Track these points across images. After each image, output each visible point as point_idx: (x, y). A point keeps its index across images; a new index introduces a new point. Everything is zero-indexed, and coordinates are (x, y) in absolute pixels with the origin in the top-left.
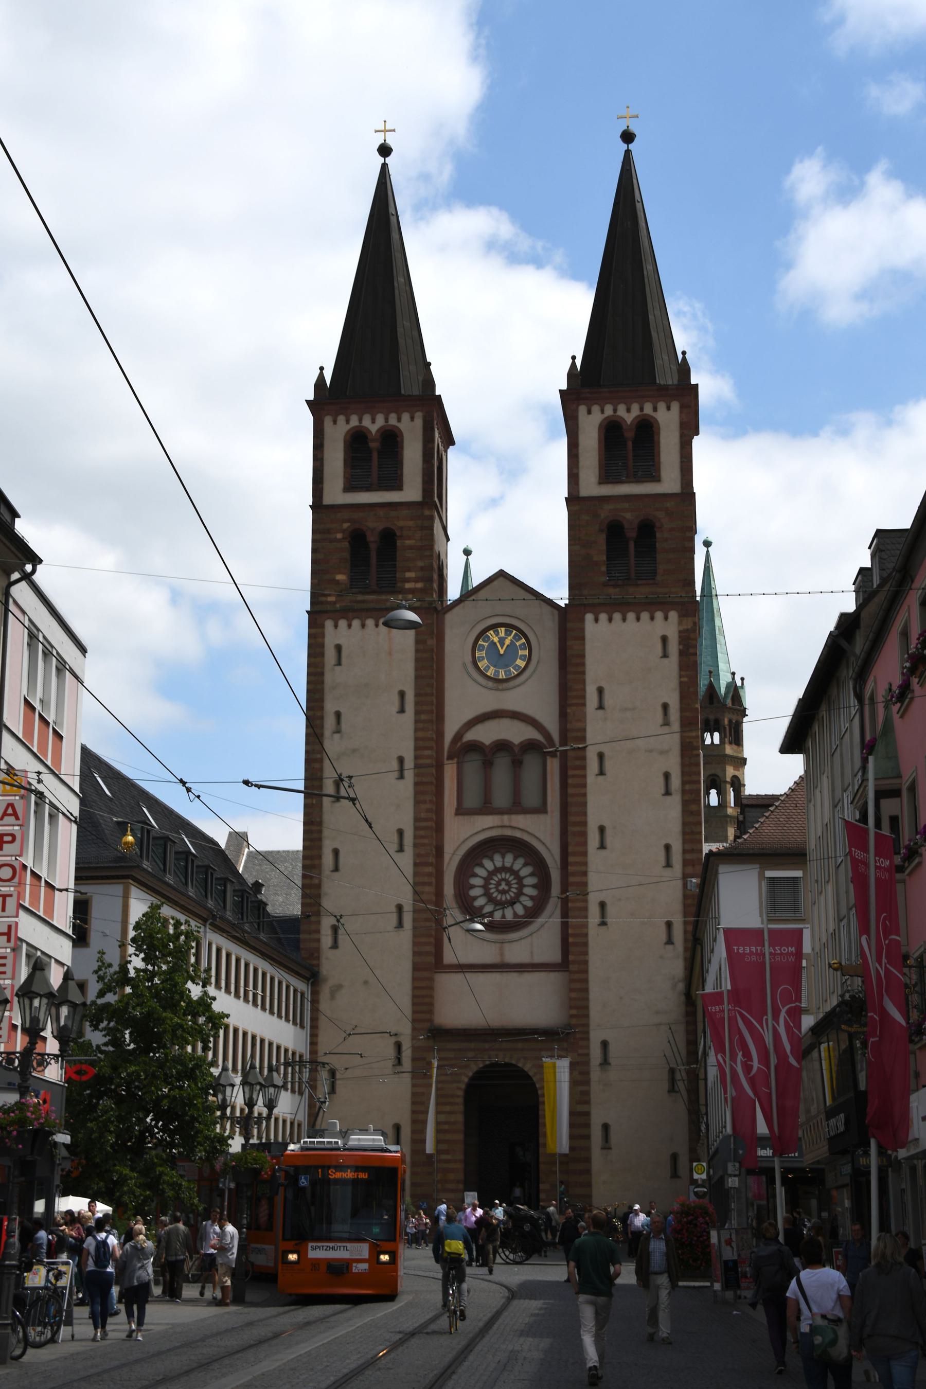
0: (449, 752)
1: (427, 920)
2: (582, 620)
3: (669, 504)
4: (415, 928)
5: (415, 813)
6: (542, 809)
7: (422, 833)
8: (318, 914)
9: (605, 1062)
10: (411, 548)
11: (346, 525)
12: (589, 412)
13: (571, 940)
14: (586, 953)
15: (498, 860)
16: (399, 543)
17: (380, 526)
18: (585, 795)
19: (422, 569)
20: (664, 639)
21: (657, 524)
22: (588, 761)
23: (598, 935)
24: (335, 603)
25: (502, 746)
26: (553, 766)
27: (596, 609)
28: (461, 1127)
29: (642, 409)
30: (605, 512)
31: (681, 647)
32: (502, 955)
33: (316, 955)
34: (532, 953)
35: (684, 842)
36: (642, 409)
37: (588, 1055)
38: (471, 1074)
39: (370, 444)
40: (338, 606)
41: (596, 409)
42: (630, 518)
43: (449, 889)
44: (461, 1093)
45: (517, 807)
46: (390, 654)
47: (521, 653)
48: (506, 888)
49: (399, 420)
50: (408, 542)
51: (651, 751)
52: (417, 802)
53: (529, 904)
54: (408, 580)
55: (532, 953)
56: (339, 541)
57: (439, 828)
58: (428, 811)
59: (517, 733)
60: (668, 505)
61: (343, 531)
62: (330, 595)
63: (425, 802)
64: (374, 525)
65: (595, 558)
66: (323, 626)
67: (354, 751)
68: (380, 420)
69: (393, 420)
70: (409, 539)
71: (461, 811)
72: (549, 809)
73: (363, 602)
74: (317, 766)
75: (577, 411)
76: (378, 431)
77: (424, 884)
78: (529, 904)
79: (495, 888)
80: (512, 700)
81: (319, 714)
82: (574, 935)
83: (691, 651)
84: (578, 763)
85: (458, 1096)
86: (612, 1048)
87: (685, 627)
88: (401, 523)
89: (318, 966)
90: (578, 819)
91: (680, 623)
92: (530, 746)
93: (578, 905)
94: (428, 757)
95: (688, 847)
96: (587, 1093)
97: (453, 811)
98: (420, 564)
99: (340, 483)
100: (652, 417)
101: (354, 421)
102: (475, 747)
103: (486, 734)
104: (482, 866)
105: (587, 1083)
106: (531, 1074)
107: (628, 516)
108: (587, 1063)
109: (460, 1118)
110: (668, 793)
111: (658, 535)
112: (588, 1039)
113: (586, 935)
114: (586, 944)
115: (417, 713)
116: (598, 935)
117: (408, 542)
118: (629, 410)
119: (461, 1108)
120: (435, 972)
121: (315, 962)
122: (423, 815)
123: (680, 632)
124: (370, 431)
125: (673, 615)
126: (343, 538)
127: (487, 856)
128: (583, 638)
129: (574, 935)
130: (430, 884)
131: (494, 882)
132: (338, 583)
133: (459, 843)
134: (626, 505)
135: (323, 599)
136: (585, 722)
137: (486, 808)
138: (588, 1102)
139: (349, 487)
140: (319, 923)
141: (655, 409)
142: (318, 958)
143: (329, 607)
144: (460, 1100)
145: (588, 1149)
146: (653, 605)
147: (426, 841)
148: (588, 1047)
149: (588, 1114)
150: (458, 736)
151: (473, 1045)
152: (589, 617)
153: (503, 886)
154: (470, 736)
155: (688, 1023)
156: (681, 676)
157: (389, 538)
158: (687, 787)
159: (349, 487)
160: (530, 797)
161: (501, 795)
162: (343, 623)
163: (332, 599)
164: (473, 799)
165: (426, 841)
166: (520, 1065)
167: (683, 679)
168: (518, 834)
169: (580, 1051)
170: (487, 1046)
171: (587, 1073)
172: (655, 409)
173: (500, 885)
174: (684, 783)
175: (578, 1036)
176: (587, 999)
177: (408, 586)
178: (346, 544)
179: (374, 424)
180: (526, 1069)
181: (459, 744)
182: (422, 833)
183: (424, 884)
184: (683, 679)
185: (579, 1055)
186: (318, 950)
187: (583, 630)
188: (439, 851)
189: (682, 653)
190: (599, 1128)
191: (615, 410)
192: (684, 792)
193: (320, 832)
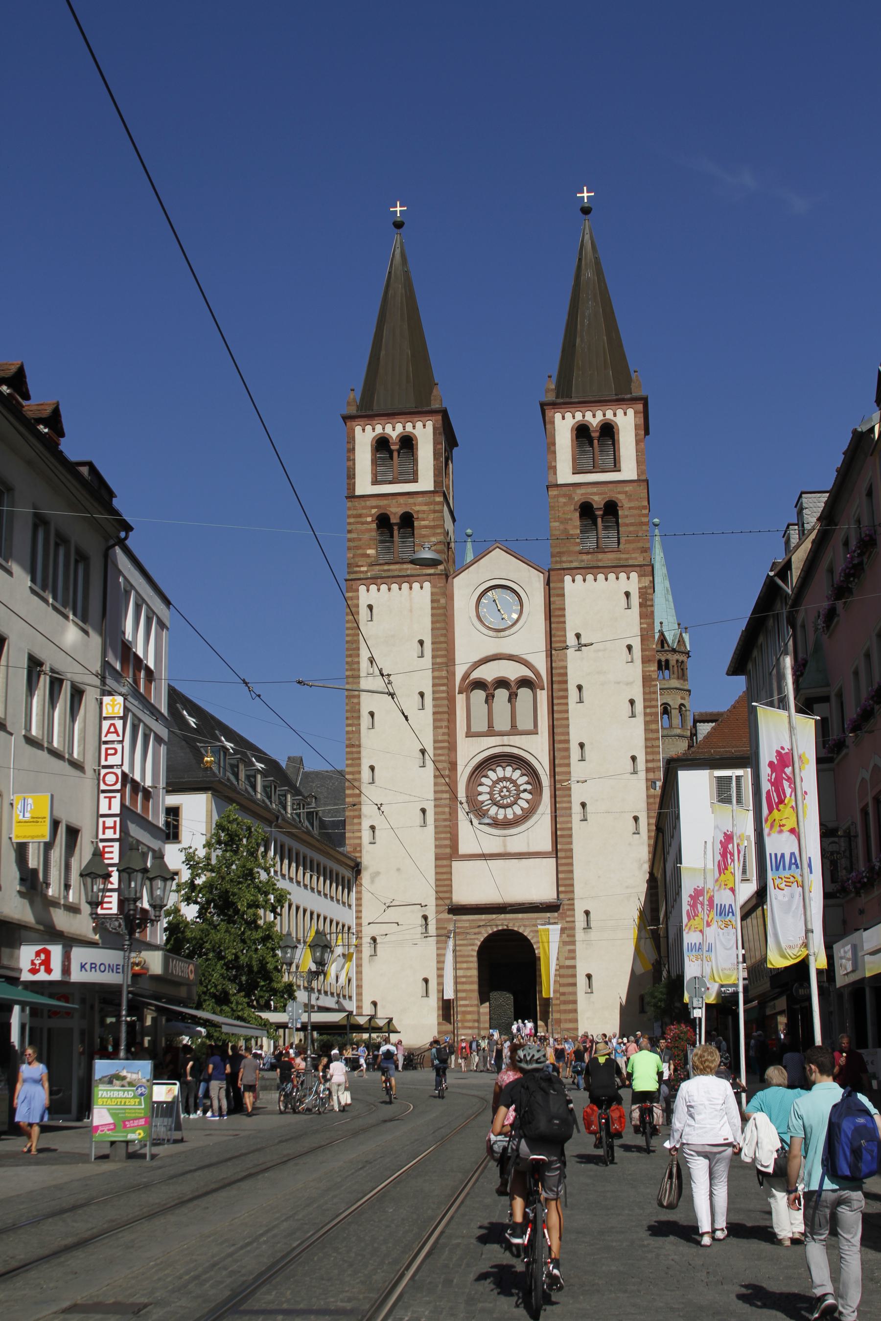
1: (445, 820)
2: (563, 581)
3: (628, 488)
4: (436, 827)
5: (434, 735)
6: (534, 732)
7: (440, 752)
8: (359, 817)
9: (588, 927)
10: (426, 527)
11: (374, 511)
12: (563, 418)
13: (559, 833)
14: (571, 843)
16: (416, 523)
17: (400, 511)
18: (567, 719)
21: (620, 505)
24: (367, 572)
25: (502, 683)
26: (543, 696)
27: (572, 571)
28: (476, 979)
29: (604, 415)
30: (579, 496)
31: (641, 600)
32: (505, 846)
33: (358, 849)
35: (647, 753)
36: (604, 415)
38: (482, 939)
40: (369, 574)
41: (568, 415)
42: (598, 501)
43: (462, 794)
44: (475, 954)
45: (514, 730)
46: (411, 611)
47: (514, 608)
49: (414, 427)
50: (423, 523)
51: (619, 683)
52: (435, 728)
53: (526, 805)
55: (528, 843)
57: (452, 747)
58: (444, 734)
59: (513, 672)
60: (627, 489)
61: (371, 515)
62: (362, 566)
63: (441, 727)
64: (395, 511)
65: (571, 532)
66: (357, 591)
68: (399, 428)
69: (409, 427)
70: (424, 520)
71: (469, 734)
73: (388, 570)
74: (355, 701)
75: (554, 417)
76: (397, 436)
77: (442, 792)
78: (526, 805)
80: (507, 645)
81: (356, 660)
82: (562, 829)
83: (649, 603)
84: (561, 693)
85: (472, 956)
86: (592, 916)
87: (644, 585)
88: (417, 508)
89: (360, 857)
90: (562, 738)
91: (639, 581)
92: (524, 682)
93: (565, 805)
94: (443, 692)
95: (650, 757)
96: (574, 951)
98: (434, 539)
99: (369, 477)
100: (613, 421)
101: (379, 429)
102: (479, 684)
103: (488, 673)
104: (486, 776)
105: (573, 943)
106: (529, 938)
107: (596, 498)
108: (573, 928)
109: (475, 973)
110: (633, 715)
111: (620, 513)
112: (574, 910)
113: (571, 829)
114: (570, 836)
115: (433, 657)
117: (423, 523)
118: (594, 416)
119: (476, 965)
121: (357, 855)
122: (440, 738)
123: (639, 588)
124: (391, 437)
125: (634, 575)
127: (491, 770)
128: (563, 595)
129: (562, 829)
132: (368, 556)
134: (595, 490)
135: (358, 569)
136: (566, 661)
137: (491, 732)
138: (574, 958)
139: (375, 482)
140: (360, 824)
141: (615, 415)
142: (360, 851)
143: (362, 576)
144: (475, 959)
145: (575, 993)
146: (618, 568)
148: (573, 916)
149: (574, 967)
150: (466, 675)
152: (568, 579)
153: (505, 792)
154: (475, 675)
156: (641, 624)
157: (407, 520)
158: (648, 710)
159: (375, 482)
160: (524, 722)
161: (502, 722)
162: (373, 588)
163: (364, 569)
164: (480, 725)
165: (443, 758)
166: (521, 931)
167: (643, 626)
169: (568, 919)
171: (574, 936)
172: (615, 415)
173: (502, 792)
174: (645, 707)
175: (566, 907)
176: (572, 879)
178: (374, 526)
179: (394, 431)
180: (525, 934)
181: (467, 681)
182: (440, 752)
183: (442, 792)
184: (643, 626)
186: (360, 845)
187: (563, 588)
188: (453, 766)
189: (641, 605)
191: (584, 416)
192: (645, 714)
193: (359, 752)
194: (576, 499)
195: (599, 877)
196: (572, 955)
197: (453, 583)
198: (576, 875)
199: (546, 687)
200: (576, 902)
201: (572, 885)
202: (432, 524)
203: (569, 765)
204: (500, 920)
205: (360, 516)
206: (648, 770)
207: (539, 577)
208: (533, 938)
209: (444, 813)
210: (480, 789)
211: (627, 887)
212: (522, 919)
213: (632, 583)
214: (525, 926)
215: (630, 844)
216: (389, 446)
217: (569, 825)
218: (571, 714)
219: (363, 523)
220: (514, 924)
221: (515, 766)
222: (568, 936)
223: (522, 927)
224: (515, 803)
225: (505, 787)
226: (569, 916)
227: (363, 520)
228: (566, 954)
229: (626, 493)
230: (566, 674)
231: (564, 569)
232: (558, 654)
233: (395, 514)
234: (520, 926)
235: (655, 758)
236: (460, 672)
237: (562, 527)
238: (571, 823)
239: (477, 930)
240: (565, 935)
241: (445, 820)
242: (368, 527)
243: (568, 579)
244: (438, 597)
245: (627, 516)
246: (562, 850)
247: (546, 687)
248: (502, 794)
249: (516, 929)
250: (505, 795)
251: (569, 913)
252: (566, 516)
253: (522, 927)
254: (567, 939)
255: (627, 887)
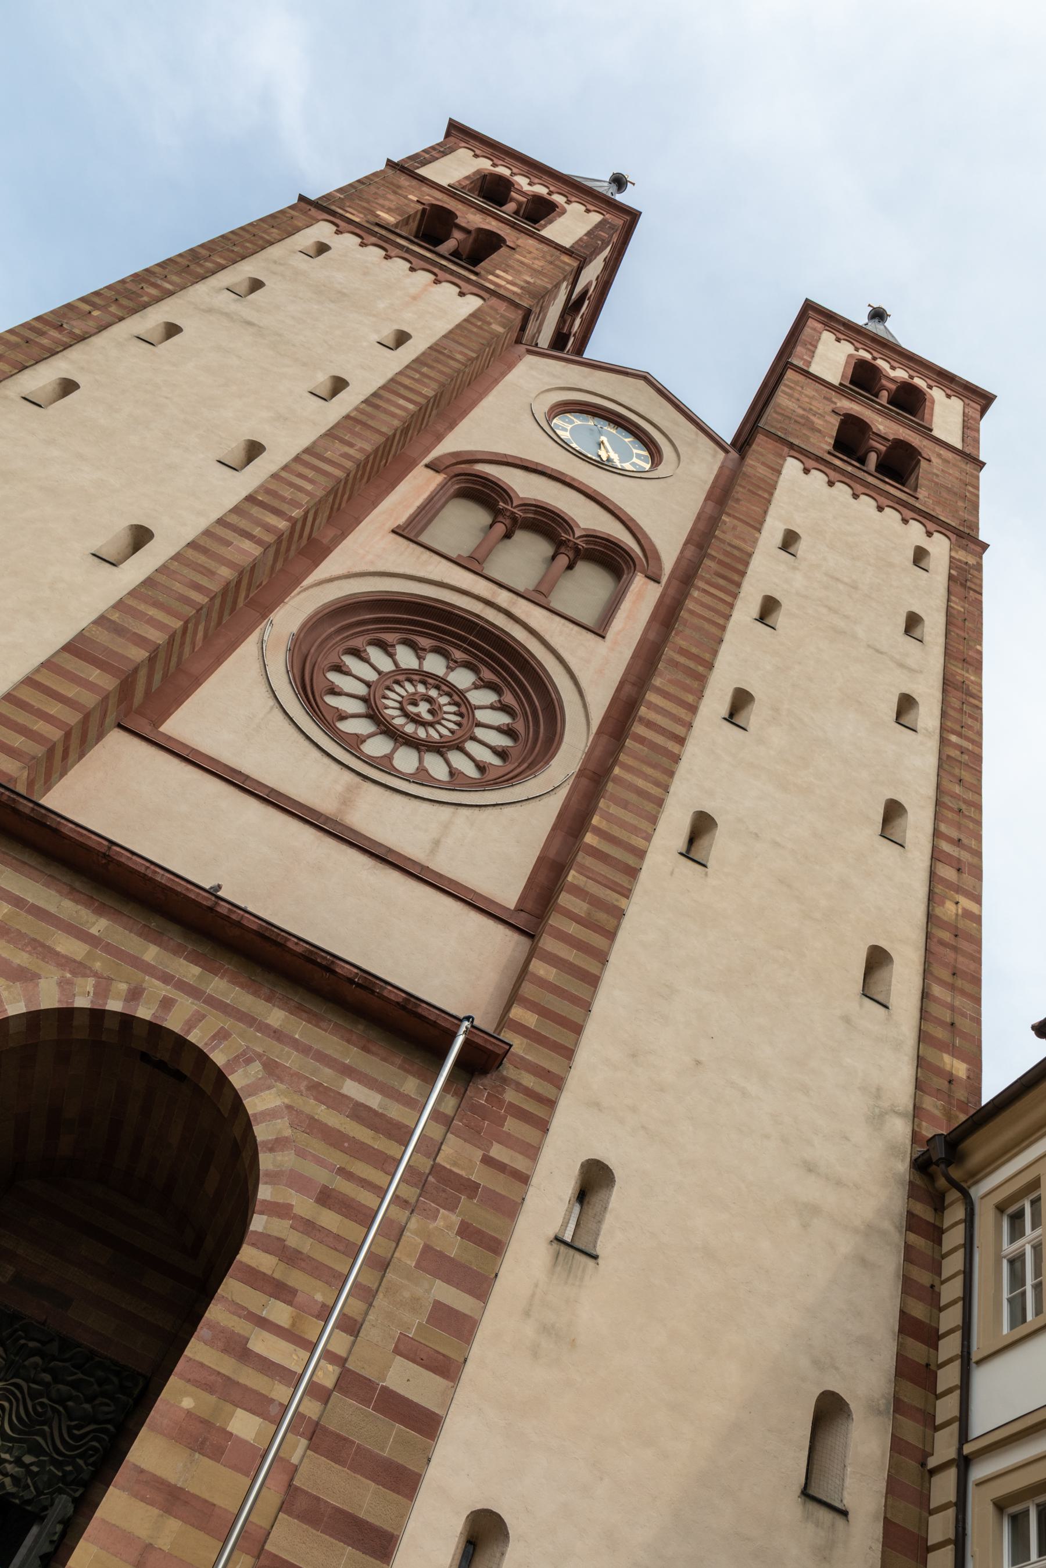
0: (437, 459)
1: (197, 587)
14: (627, 894)
15: (434, 664)
19: (528, 283)
20: (920, 556)
22: (739, 604)
23: (672, 873)
30: (847, 405)
34: (437, 843)
35: (937, 817)
37: (524, 1179)
39: (512, 193)
48: (428, 717)
50: (518, 257)
54: (498, 276)
55: (437, 843)
56: (412, 201)
63: (351, 445)
67: (250, 323)
72: (610, 634)
79: (400, 703)
82: (599, 832)
97: (393, 524)
98: (528, 279)
106: (261, 1132)
107: (881, 427)
108: (511, 1209)
112: (543, 1126)
113: (641, 854)
114: (633, 873)
116: (672, 873)
117: (518, 257)
120: (120, 726)
122: (328, 454)
126: (418, 201)
129: (599, 832)
130: (259, 542)
131: (404, 693)
132: (378, 216)
133: (372, 569)
136: (754, 547)
147: (309, 487)
148: (533, 1152)
151: (99, 925)
153: (423, 709)
155: (910, 1254)
165: (309, 487)
166: (238, 1080)
168: (519, 634)
169: (498, 1152)
170: (151, 953)
171: (496, 1247)
173: (415, 704)
175: (510, 1096)
177: (491, 277)
180: (253, 1105)
185: (488, 1161)
187: (782, 466)
190: (455, 1527)
194: (839, 404)
195: (698, 1063)
196: (443, 1343)
197: (520, 358)
198: (601, 1004)
199: (664, 580)
200: (566, 1102)
201: (577, 1029)
202: (535, 266)
203: (693, 709)
204: (166, 979)
205: (399, 187)
206: (936, 856)
207: (714, 456)
208: (279, 1144)
209: (210, 573)
210: (351, 662)
211: (810, 1168)
212: (277, 1035)
213: (939, 547)
214: (272, 1069)
215: (847, 1020)
216: (510, 191)
217: (638, 842)
218: (731, 625)
219: (395, 193)
220: (222, 1035)
221: (488, 675)
222: (466, 1231)
223: (256, 1068)
224: (439, 749)
225: (429, 700)
226: (508, 1141)
227: (400, 192)
228: (414, 1322)
229: (939, 456)
230: (747, 564)
231: (791, 446)
232: (734, 528)
233: (468, 222)
234: (245, 1058)
235: (965, 841)
236: (457, 441)
237: (801, 412)
238: (648, 838)
239: (21, 958)
240: (455, 1219)
241: (197, 587)
242: (406, 201)
243: (792, 467)
244: (492, 321)
245: (937, 476)
246: (578, 892)
247: (664, 580)
248: (411, 709)
249: (219, 1058)
250: (418, 715)
251: (512, 1125)
252: (814, 408)
253: (256, 1068)
254: (453, 1246)
255: (810, 1168)
